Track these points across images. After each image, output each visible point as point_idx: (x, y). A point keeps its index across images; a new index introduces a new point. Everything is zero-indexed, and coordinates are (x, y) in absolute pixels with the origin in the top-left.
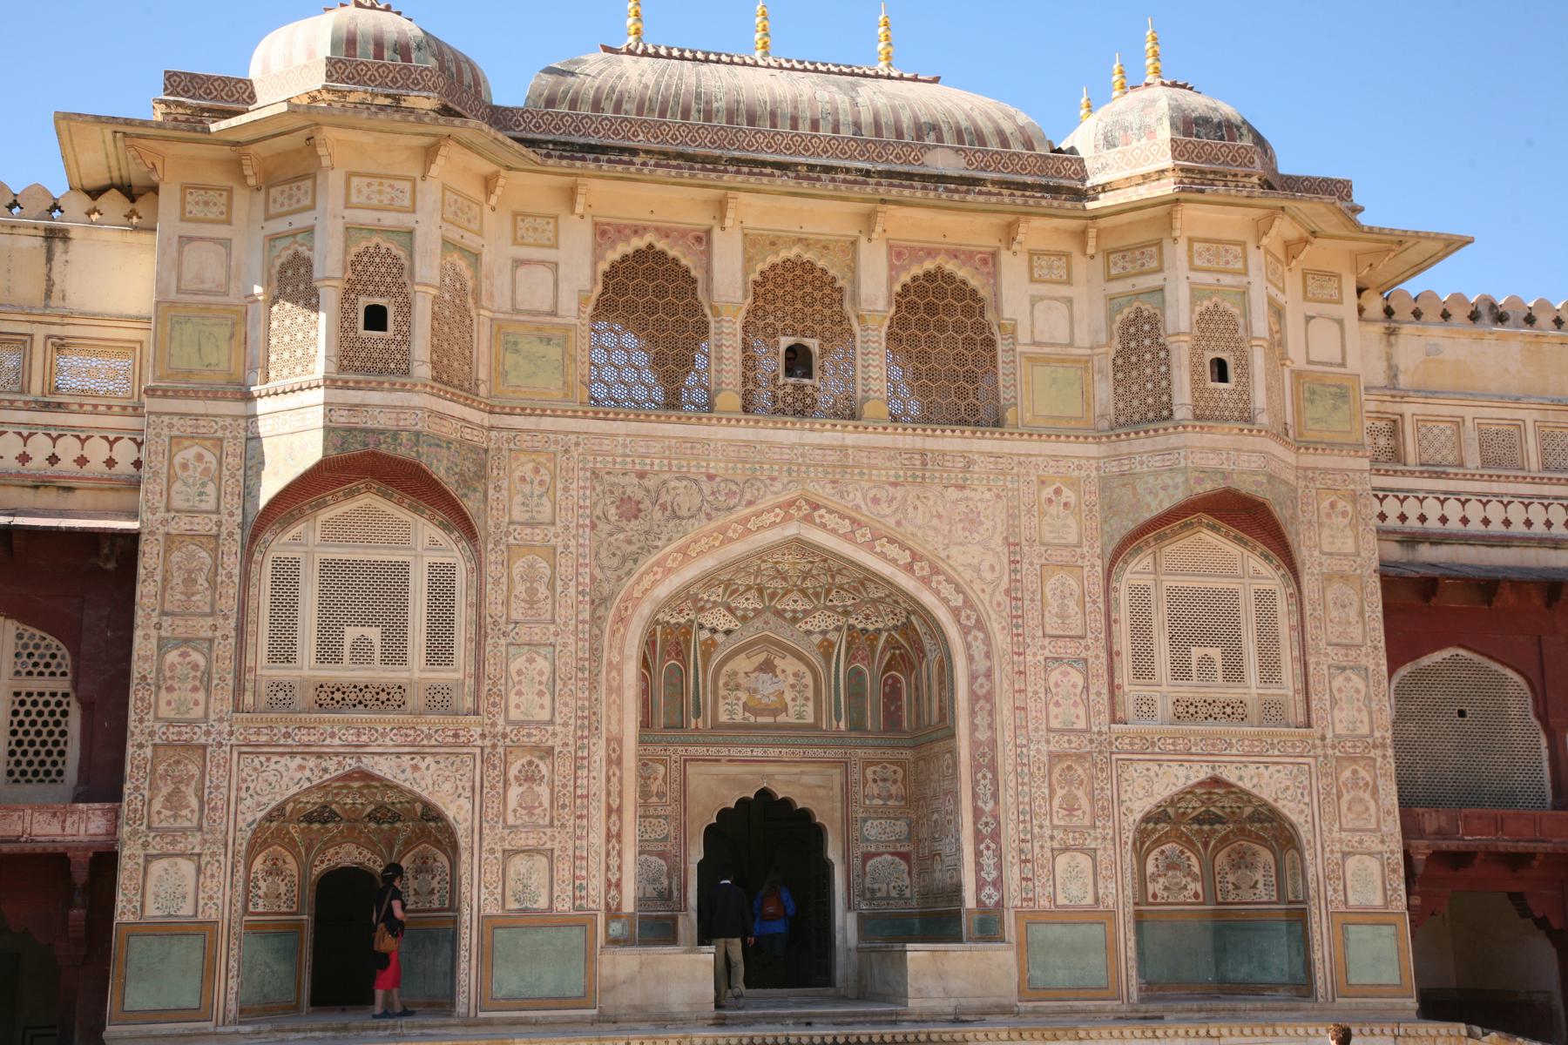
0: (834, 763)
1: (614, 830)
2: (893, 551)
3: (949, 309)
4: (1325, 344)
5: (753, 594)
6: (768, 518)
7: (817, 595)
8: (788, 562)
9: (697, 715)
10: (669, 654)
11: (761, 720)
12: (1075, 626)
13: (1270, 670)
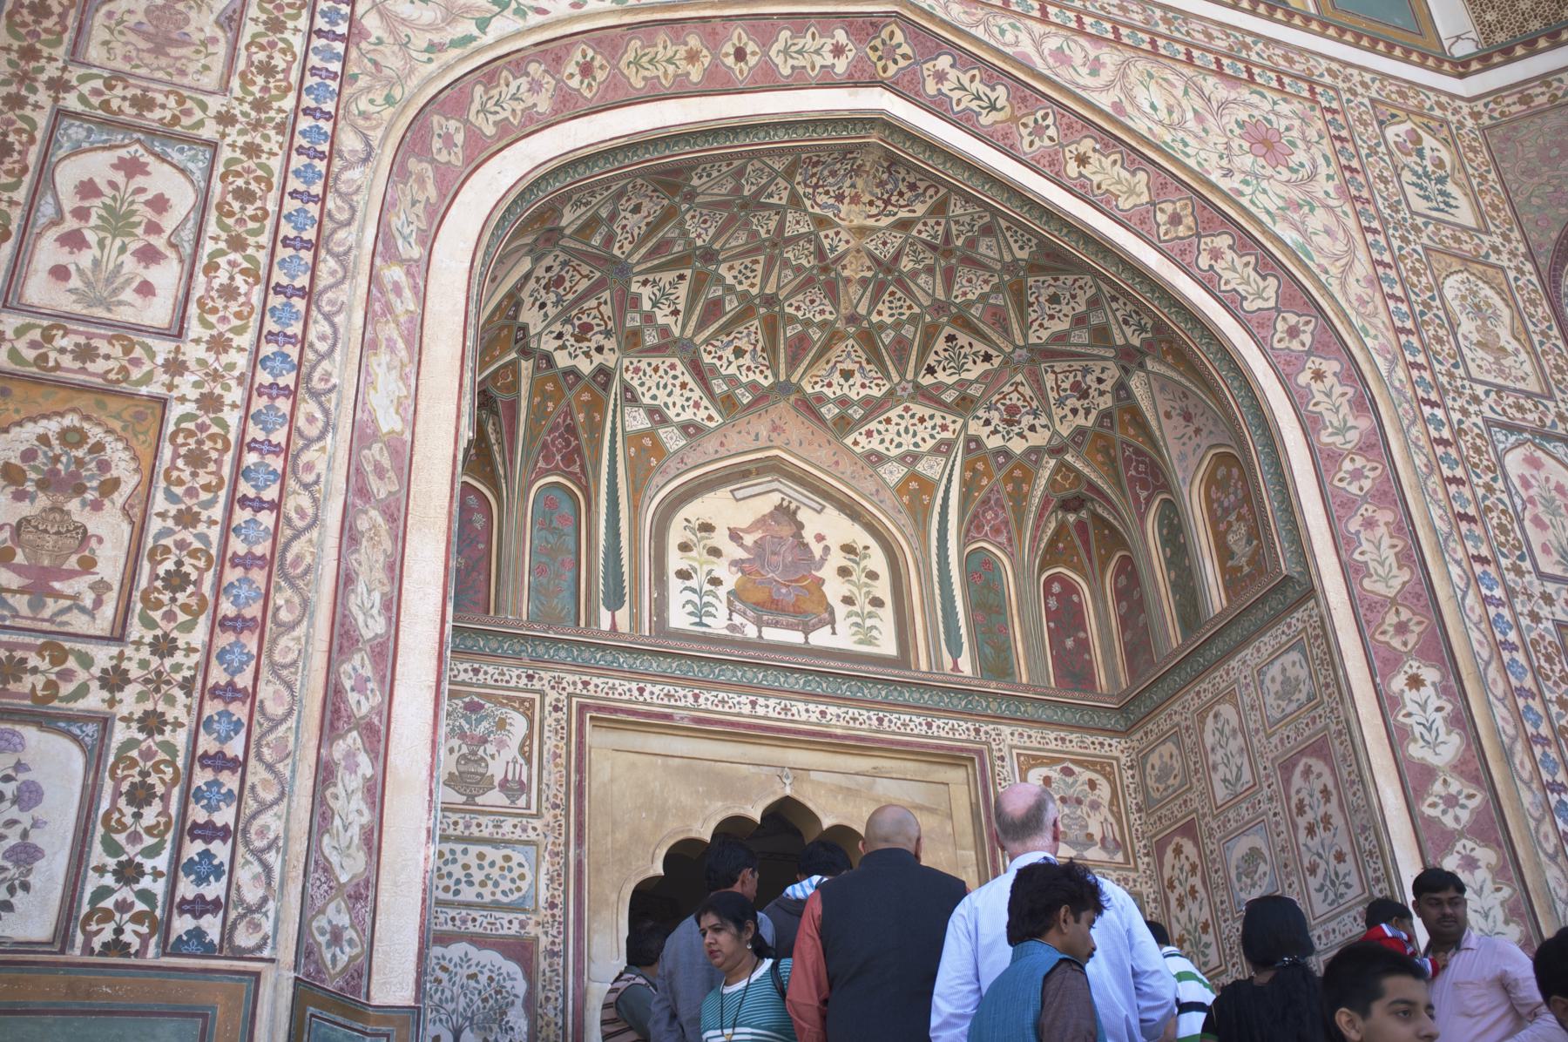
0: (954, 757)
1: (362, 704)
2: (1106, 171)
5: (751, 334)
6: (818, 50)
7: (900, 349)
9: (614, 603)
10: (547, 459)
11: (772, 634)
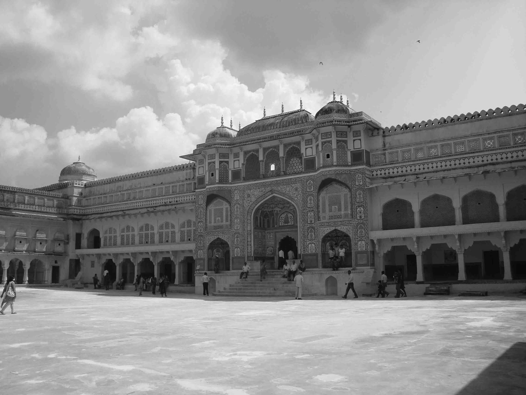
3: (295, 153)
4: (357, 145)
8: (279, 199)
12: (313, 205)
13: (346, 208)
